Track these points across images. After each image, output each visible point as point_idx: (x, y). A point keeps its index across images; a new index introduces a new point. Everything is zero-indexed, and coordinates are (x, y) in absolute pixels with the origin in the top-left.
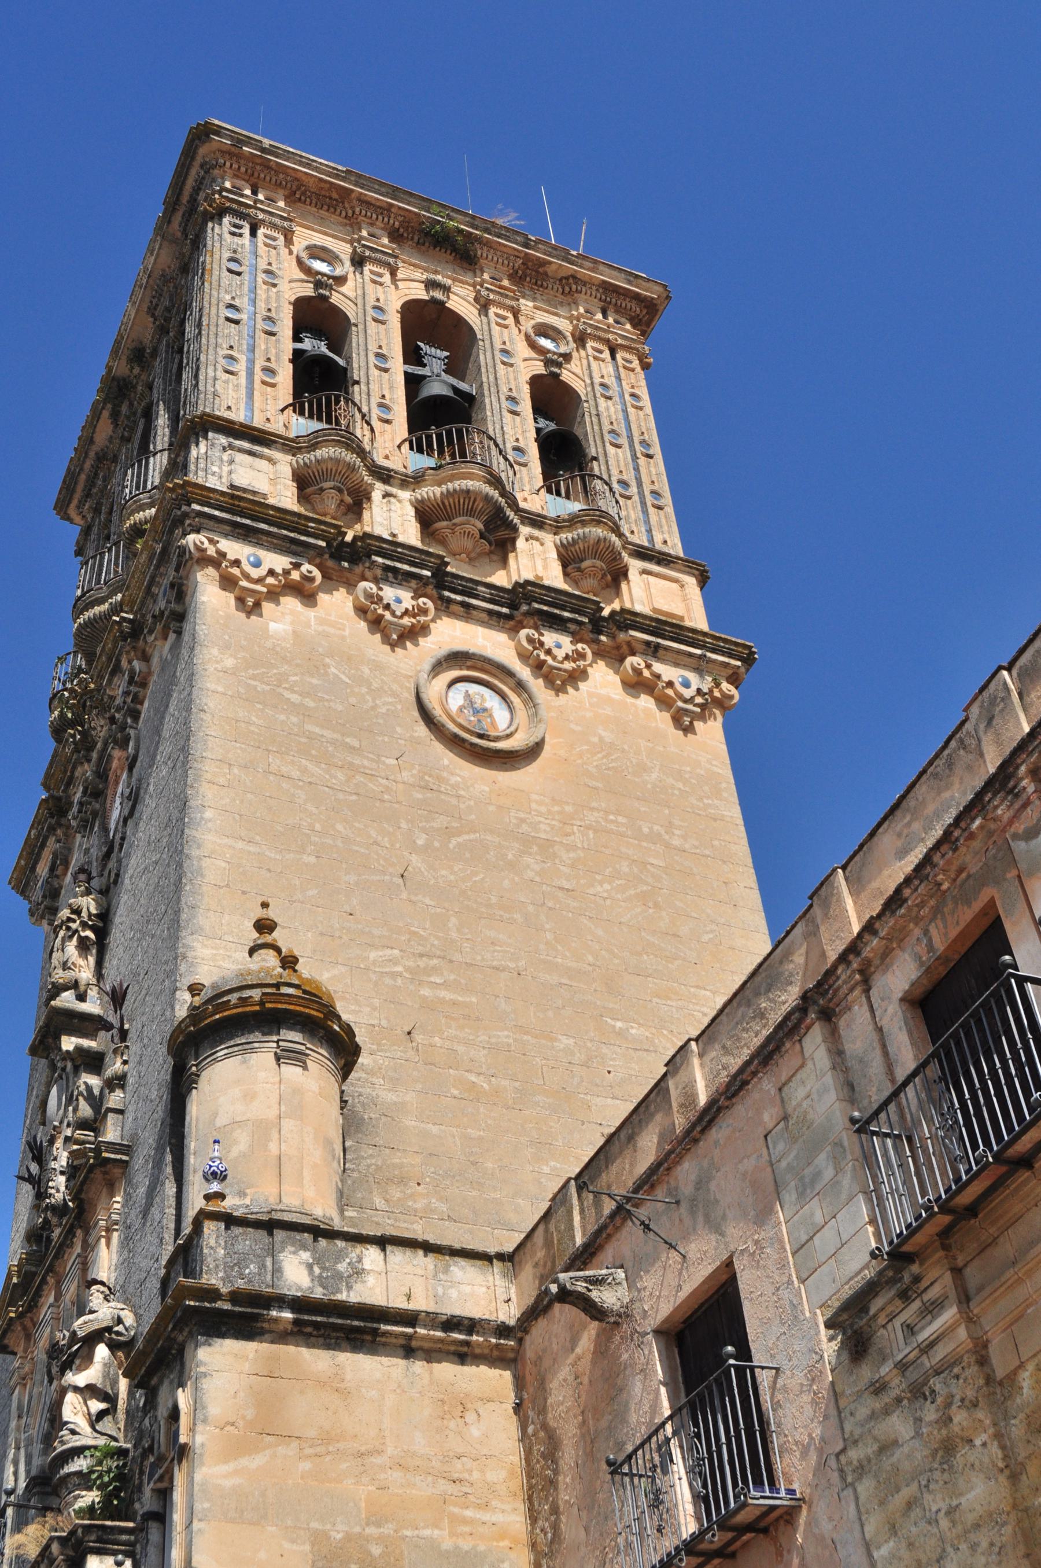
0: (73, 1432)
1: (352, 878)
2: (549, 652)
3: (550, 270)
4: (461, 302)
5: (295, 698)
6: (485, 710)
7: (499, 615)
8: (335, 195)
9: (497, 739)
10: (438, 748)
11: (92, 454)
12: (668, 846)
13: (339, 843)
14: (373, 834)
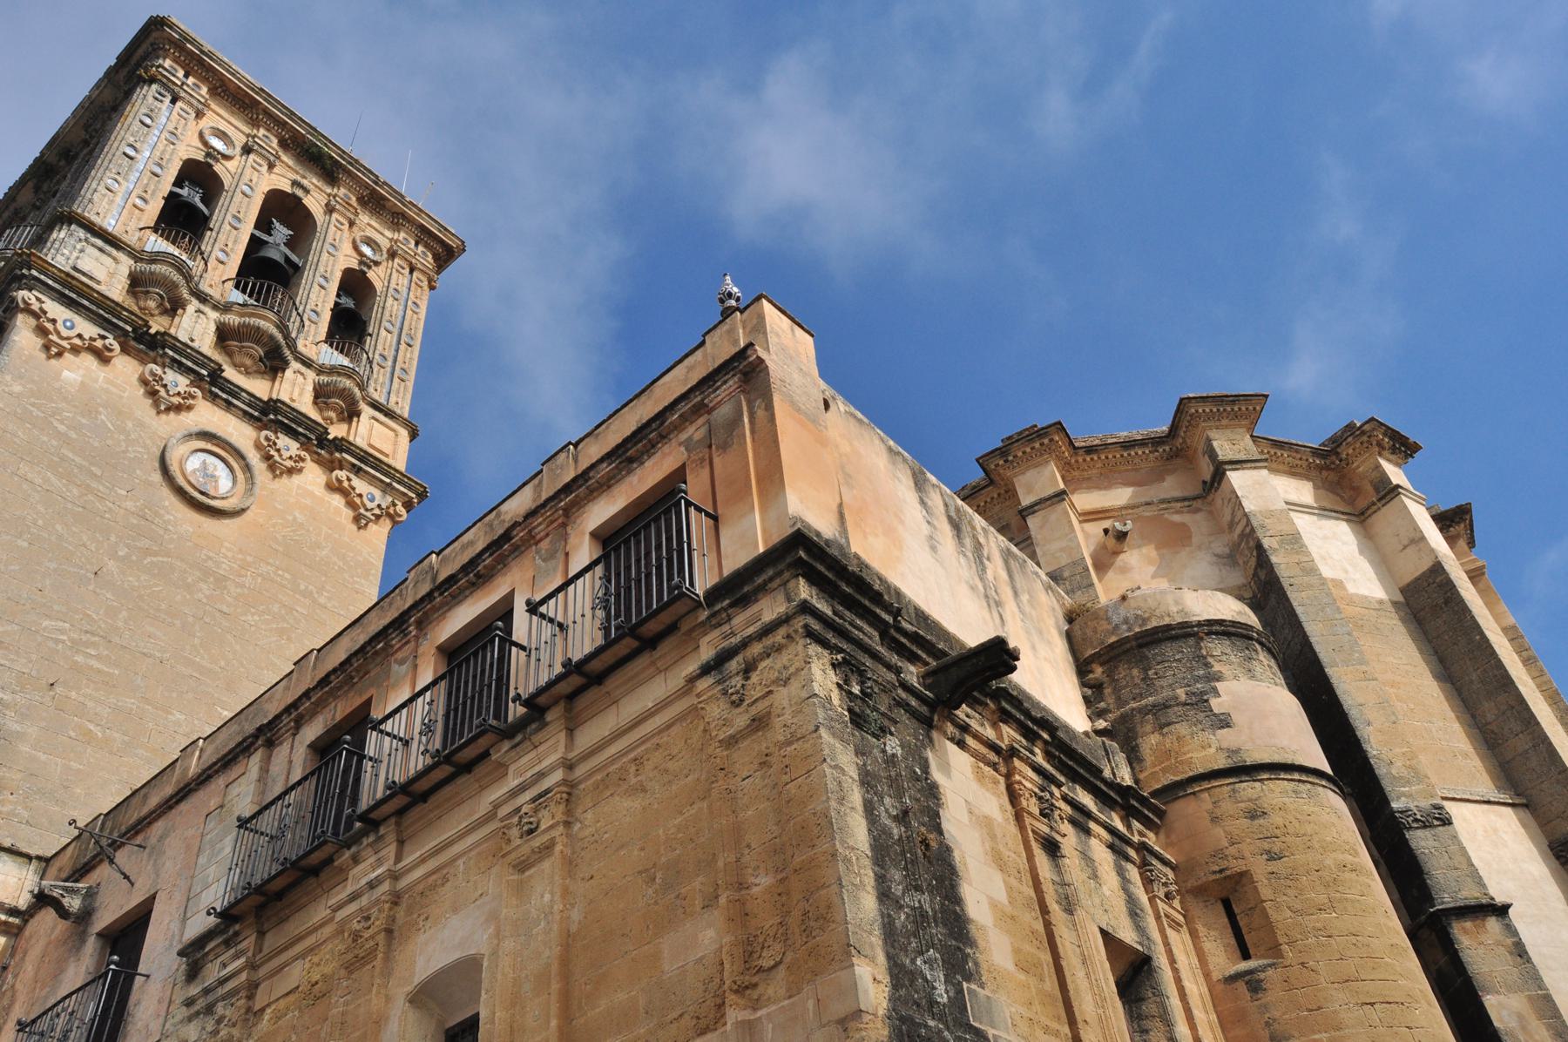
1: (53, 565)
2: (278, 450)
3: (388, 205)
4: (314, 203)
5: (62, 428)
6: (213, 476)
7: (252, 416)
9: (214, 498)
11: (12, 208)
12: (314, 601)
13: (53, 538)
14: (85, 538)
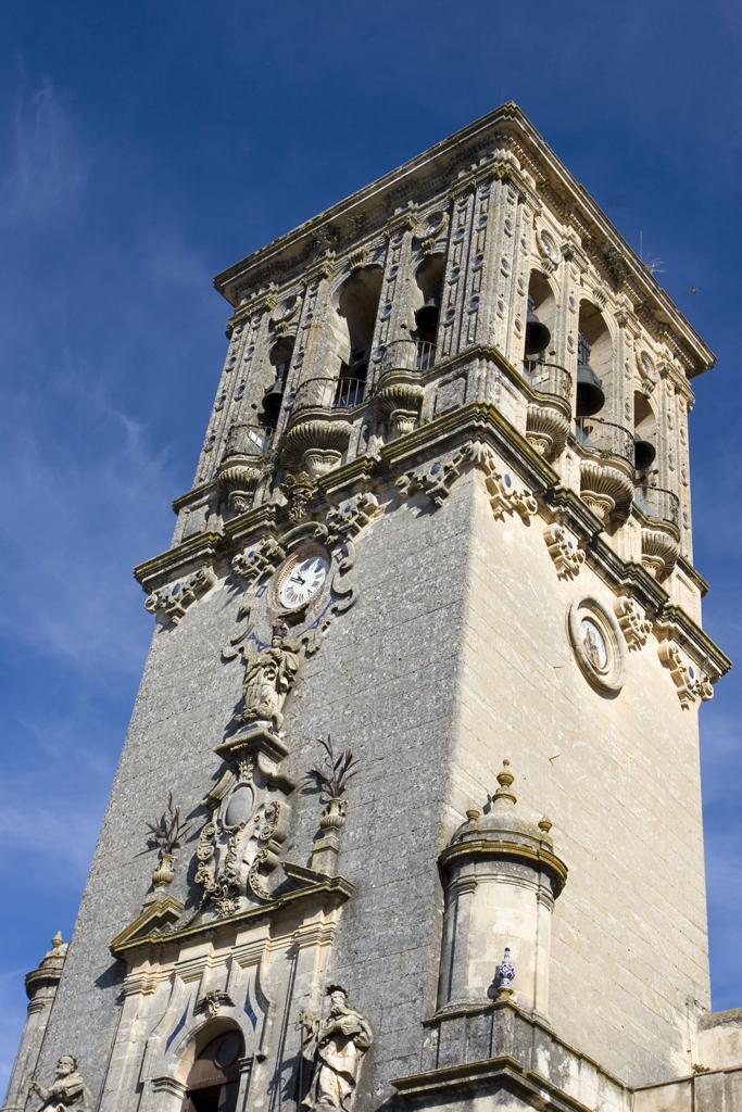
0: (331, 1103)
3: (658, 314)
5: (511, 595)
8: (563, 197)
9: (600, 673)
10: (574, 664)
